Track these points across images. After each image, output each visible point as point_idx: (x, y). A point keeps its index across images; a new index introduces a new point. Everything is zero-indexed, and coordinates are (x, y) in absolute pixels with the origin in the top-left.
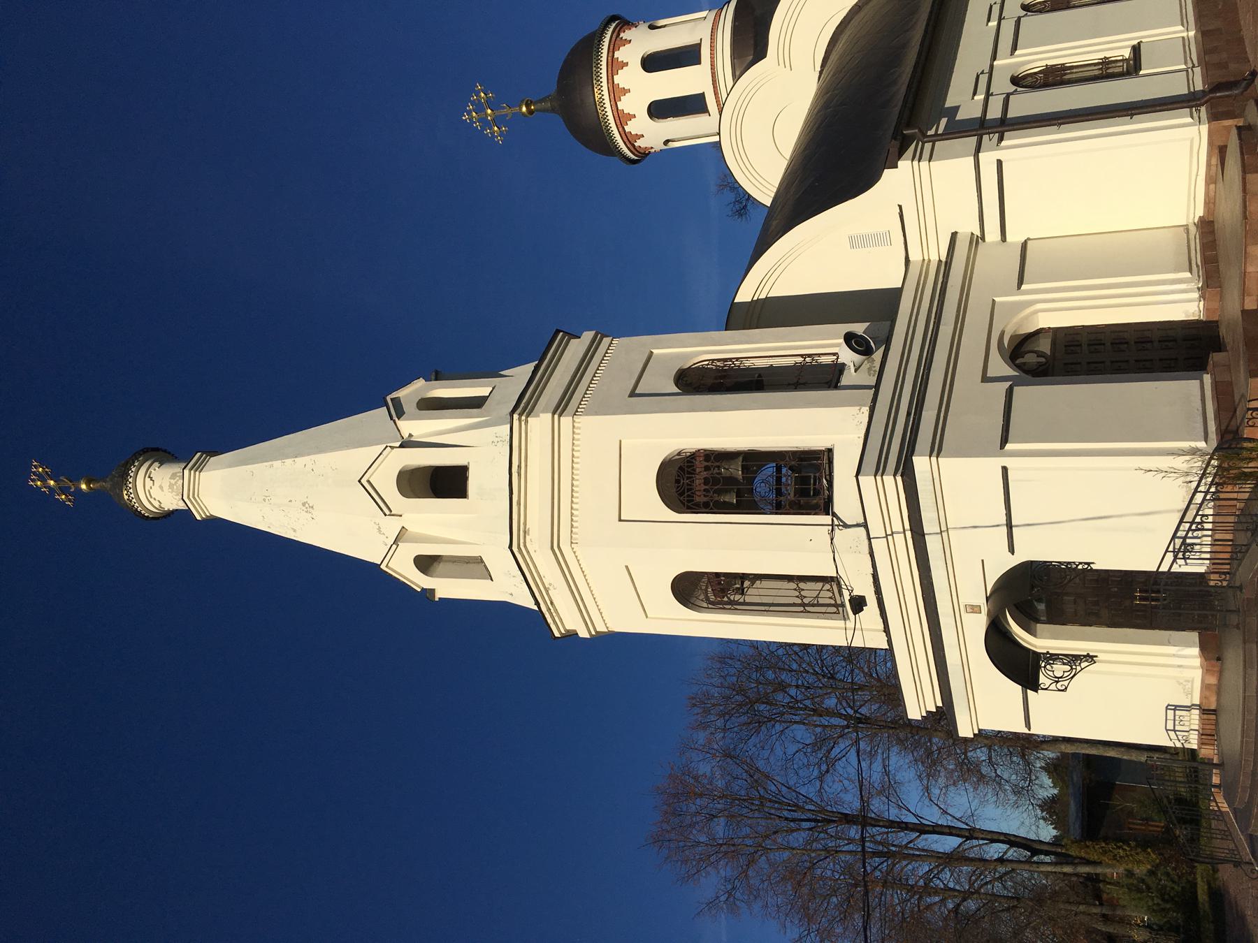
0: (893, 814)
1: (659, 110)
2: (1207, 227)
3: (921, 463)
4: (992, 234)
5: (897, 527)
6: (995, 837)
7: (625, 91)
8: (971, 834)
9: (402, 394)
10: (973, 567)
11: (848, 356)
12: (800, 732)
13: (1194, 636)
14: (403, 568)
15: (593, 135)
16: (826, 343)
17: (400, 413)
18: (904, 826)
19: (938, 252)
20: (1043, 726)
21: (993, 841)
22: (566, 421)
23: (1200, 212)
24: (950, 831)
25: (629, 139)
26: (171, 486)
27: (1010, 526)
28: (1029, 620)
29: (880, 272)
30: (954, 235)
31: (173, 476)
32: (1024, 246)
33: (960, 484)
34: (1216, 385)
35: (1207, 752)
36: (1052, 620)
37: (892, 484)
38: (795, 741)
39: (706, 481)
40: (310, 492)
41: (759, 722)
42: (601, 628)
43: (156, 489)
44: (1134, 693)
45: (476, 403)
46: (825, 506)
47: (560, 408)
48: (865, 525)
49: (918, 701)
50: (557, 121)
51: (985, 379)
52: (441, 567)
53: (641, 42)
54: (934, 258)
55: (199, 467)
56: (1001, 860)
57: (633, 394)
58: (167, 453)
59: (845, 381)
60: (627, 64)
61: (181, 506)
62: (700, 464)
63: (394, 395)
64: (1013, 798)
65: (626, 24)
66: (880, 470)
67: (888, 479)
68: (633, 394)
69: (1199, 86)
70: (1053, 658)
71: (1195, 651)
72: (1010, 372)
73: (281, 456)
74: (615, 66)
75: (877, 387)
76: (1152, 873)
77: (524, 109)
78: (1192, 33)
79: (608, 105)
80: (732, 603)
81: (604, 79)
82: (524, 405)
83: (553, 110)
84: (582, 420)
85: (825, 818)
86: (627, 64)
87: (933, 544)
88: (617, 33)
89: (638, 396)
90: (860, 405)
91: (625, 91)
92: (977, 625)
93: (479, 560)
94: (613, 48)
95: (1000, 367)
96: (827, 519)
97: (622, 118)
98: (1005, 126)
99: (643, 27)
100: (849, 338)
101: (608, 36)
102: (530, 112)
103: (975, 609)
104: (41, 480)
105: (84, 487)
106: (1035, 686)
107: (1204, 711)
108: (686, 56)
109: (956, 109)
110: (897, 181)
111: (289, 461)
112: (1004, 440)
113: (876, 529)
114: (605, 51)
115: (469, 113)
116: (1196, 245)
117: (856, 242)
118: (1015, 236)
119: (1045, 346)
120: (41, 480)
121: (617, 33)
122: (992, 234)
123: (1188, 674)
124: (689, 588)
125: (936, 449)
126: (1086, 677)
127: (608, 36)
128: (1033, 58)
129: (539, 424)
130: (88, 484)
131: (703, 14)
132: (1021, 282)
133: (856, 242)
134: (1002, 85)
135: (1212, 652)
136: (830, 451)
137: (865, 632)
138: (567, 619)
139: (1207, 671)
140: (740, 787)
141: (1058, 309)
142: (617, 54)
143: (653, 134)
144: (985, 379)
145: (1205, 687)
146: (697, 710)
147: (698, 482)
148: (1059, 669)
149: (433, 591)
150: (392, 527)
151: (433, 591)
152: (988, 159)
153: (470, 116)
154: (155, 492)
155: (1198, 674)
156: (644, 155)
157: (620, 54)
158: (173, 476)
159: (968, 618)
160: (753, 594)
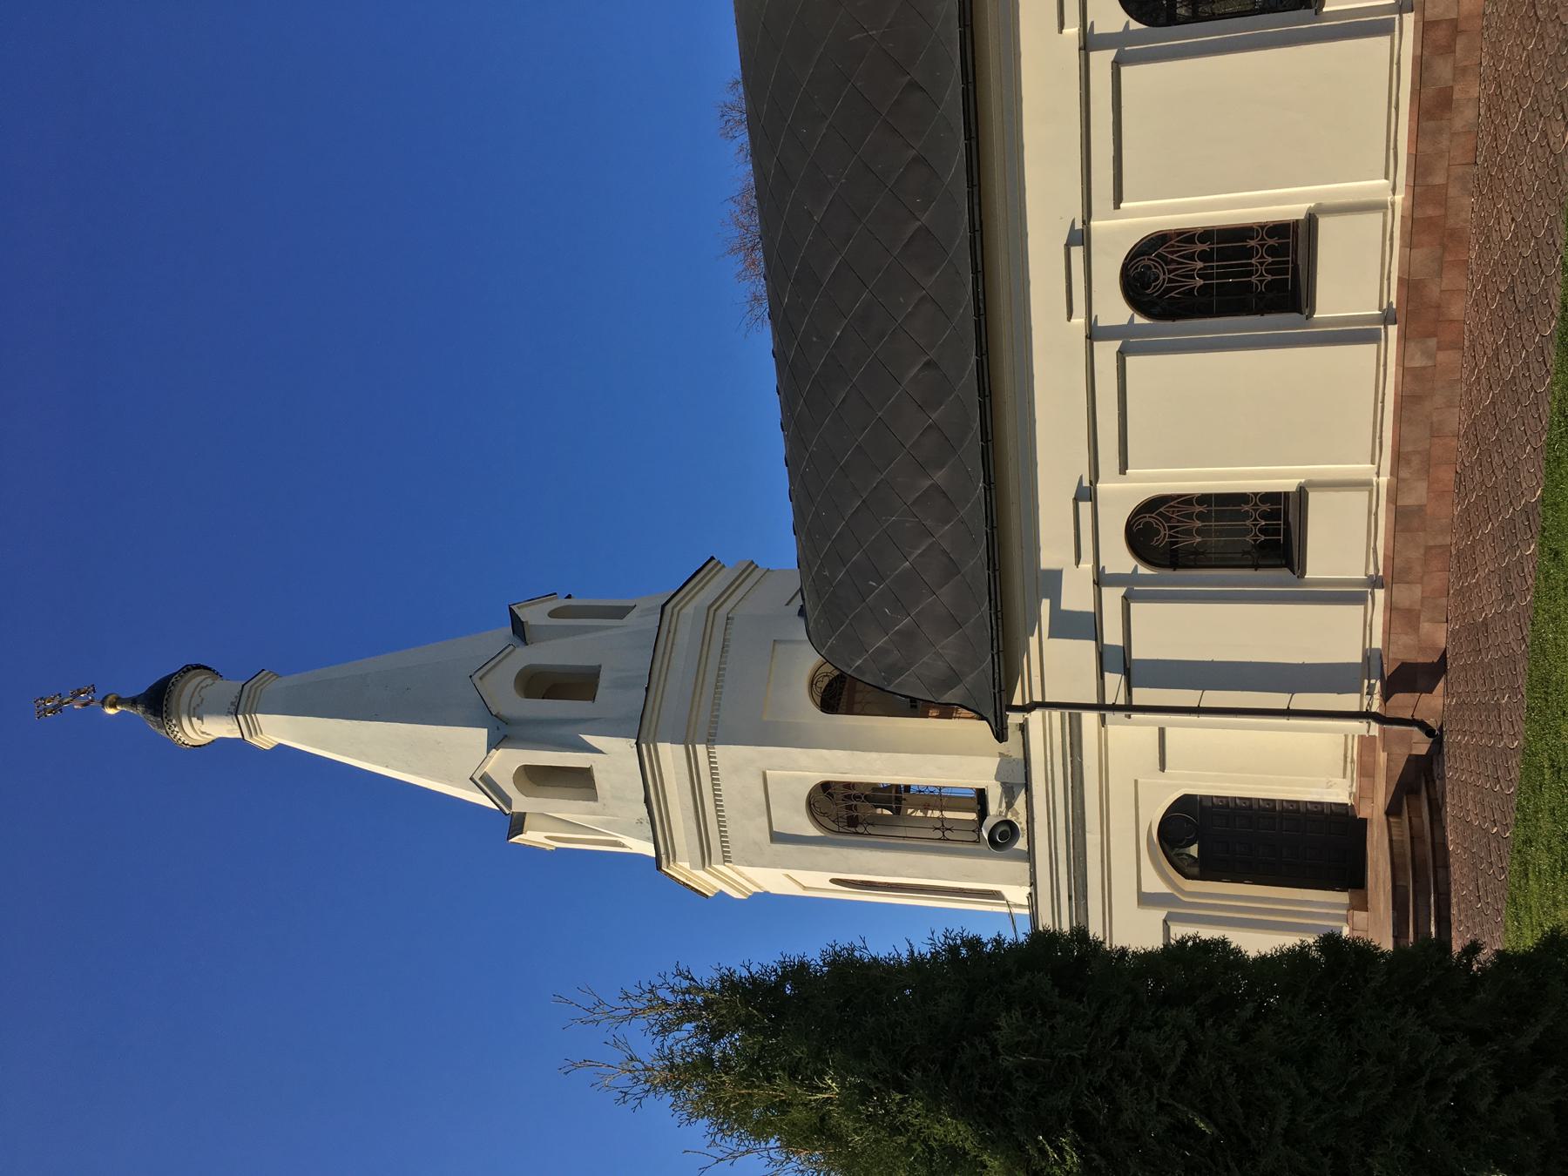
22: (720, 867)
51: (1145, 900)
68: (777, 837)
69: (1377, 643)
75: (1030, 856)
78: (1384, 480)
90: (1021, 885)
95: (1154, 883)
105: (111, 711)
109: (1057, 575)
130: (113, 706)
132: (1163, 767)
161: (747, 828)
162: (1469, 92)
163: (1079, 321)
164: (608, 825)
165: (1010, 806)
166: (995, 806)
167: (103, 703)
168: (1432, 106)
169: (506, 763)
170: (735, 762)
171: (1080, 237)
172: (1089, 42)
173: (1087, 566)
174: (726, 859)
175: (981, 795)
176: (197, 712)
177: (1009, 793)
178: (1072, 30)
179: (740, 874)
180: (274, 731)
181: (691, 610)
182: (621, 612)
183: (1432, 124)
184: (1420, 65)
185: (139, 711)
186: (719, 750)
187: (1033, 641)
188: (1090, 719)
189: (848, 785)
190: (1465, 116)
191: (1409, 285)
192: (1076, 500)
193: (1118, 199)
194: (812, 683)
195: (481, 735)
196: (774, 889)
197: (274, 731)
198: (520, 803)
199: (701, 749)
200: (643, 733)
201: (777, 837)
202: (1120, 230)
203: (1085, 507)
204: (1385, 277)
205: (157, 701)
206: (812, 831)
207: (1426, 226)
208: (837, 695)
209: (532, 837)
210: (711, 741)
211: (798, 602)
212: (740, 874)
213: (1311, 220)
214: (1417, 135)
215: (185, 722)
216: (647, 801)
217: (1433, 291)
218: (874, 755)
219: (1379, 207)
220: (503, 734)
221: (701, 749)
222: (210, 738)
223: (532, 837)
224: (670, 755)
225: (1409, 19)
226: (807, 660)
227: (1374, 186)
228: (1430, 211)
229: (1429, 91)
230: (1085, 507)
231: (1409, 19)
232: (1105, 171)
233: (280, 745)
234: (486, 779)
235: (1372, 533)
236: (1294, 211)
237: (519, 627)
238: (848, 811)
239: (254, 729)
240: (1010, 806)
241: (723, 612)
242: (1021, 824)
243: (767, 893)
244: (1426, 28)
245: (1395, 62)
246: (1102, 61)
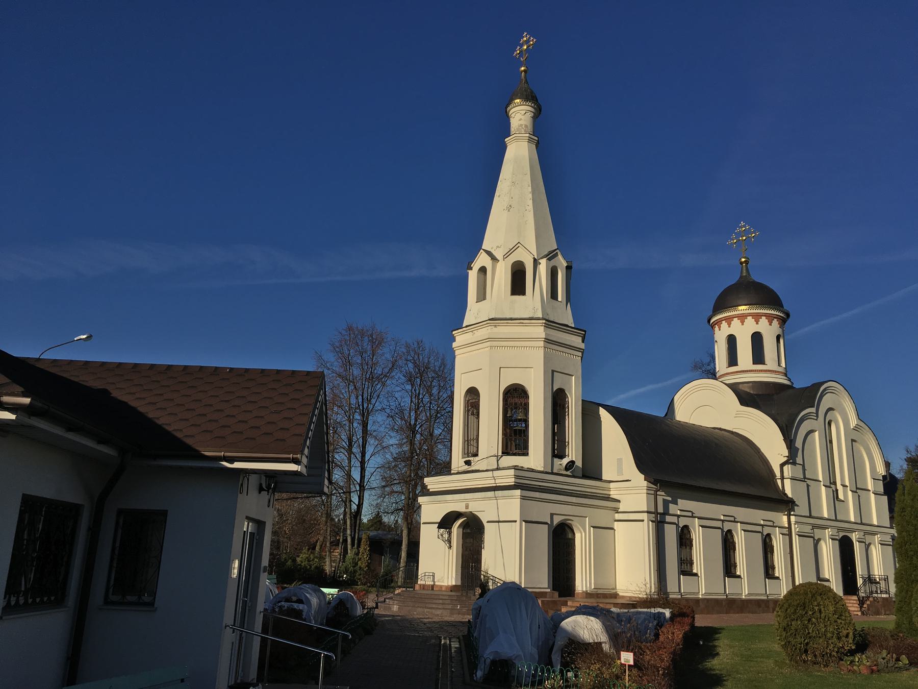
0: (370, 450)
1: (732, 341)
2: (615, 596)
3: (518, 492)
4: (617, 516)
5: (497, 481)
6: (361, 498)
7: (743, 323)
8: (362, 488)
9: (560, 256)
10: (482, 507)
11: (565, 461)
12: (406, 402)
13: (459, 583)
14: (482, 260)
15: (723, 302)
16: (574, 452)
17: (551, 256)
18: (363, 454)
19: (614, 494)
20: (424, 529)
21: (359, 497)
22: (542, 344)
23: (621, 594)
24: (362, 477)
25: (718, 323)
26: (521, 125)
27: (499, 522)
28: (464, 526)
29: (608, 471)
30: (619, 501)
31: (526, 126)
32: (612, 529)
33: (511, 505)
34: (546, 593)
35: (417, 587)
36: (463, 533)
37: (511, 481)
38: (402, 397)
39: (516, 404)
40: (515, 219)
41: (410, 379)
42: (457, 353)
43: (520, 115)
44: (438, 563)
45: (554, 295)
46: (506, 452)
47: (547, 341)
48: (498, 469)
49: (432, 483)
50: (733, 280)
51: (552, 515)
52: (482, 276)
53: (769, 330)
54: (611, 493)
55: (530, 140)
56: (351, 501)
57: (553, 371)
58: (537, 116)
59: (556, 460)
61: (512, 129)
62: (523, 401)
63: (559, 254)
64: (374, 503)
65: (783, 321)
66: (516, 477)
67: (513, 480)
68: (553, 371)
70: (450, 533)
71: (454, 584)
72: (555, 523)
73: (533, 192)
74: (757, 317)
75: (552, 473)
76: (360, 568)
77: (743, 260)
79: (736, 313)
80: (468, 411)
81: (752, 311)
82: (550, 324)
83: (741, 277)
84: (542, 351)
85: (365, 415)
87: (490, 494)
88: (777, 317)
89: (551, 374)
91: (743, 323)
92: (461, 508)
93: (484, 299)
94: (766, 315)
95: (557, 520)
96: (500, 454)
97: (729, 320)
98: (659, 521)
99: (779, 331)
100: (573, 462)
101: (775, 313)
102: (741, 263)
103: (467, 507)
104: (527, 41)
106: (439, 527)
107: (433, 586)
108: (758, 357)
110: (639, 480)
111: (531, 196)
112: (526, 522)
113: (496, 473)
114: (766, 311)
115: (744, 226)
116: (606, 592)
117: (620, 461)
118: (616, 525)
119: (570, 536)
120: (527, 41)
122: (617, 516)
123: (446, 581)
124: (473, 393)
125: (523, 498)
126: (443, 546)
128: (697, 535)
129: (539, 331)
130: (525, 71)
131: (783, 365)
133: (620, 461)
134: (683, 522)
135: (454, 588)
136: (527, 454)
137: (457, 461)
138: (461, 338)
139: (447, 587)
140: (378, 371)
141: (582, 541)
142: (764, 318)
143: (721, 335)
144: (552, 515)
145: (441, 587)
146: (416, 344)
147: (517, 400)
148: (446, 536)
149: (471, 269)
150: (499, 255)
151: (471, 269)
152: (645, 516)
153: (743, 226)
154: (518, 116)
155: (446, 584)
156: (713, 327)
157: (764, 320)
158: (526, 126)
159: (464, 504)
160: (471, 418)
173: (679, 513)
187: (663, 493)
215: (533, 110)
216: (567, 326)
221: (580, 354)
230: (690, 514)
234: (556, 255)
235: (690, 593)
246: (759, 529)
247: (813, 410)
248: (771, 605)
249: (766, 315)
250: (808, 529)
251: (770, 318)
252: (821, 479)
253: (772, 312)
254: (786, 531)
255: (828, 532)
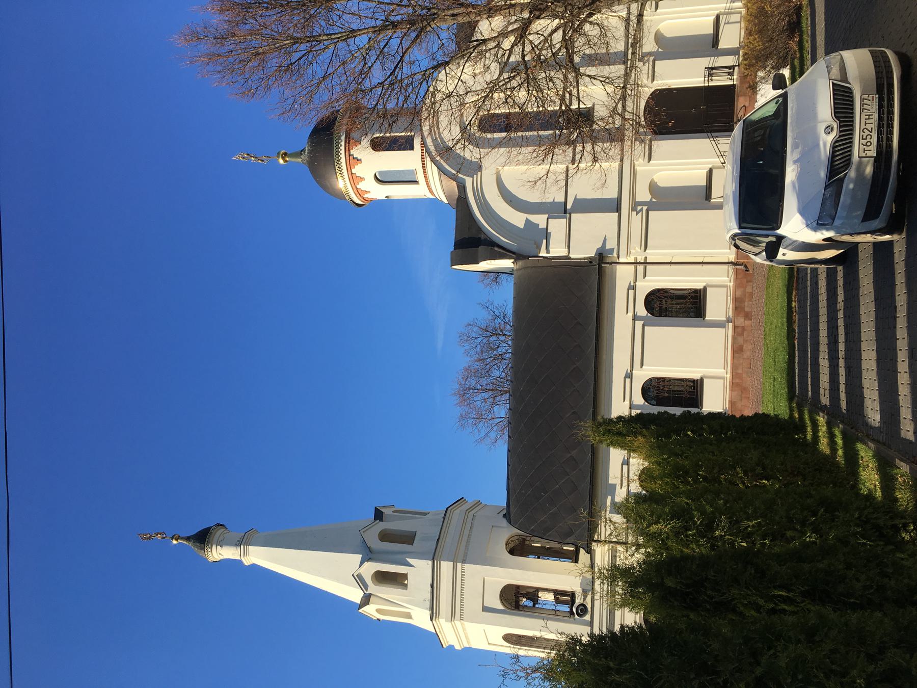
22: (458, 623)
60: (362, 179)
68: (485, 609)
81: (345, 170)
86: (362, 179)
88: (348, 150)
94: (349, 168)
101: (343, 156)
105: (175, 542)
121: (348, 150)
127: (343, 156)
130: (177, 540)
157: (357, 170)
161: (472, 603)
162: (747, 347)
163: (627, 402)
164: (409, 602)
165: (584, 599)
166: (578, 601)
167: (172, 538)
168: (737, 350)
169: (371, 568)
170: (473, 572)
171: (629, 376)
172: (635, 318)
174: (461, 619)
175: (573, 595)
176: (221, 544)
177: (585, 593)
178: (630, 314)
179: (464, 629)
180: (258, 556)
181: (457, 514)
182: (425, 514)
183: (736, 355)
184: (734, 338)
185: (189, 544)
186: (467, 566)
188: (620, 548)
189: (518, 587)
190: (747, 354)
191: (732, 403)
192: (622, 465)
193: (642, 365)
194: (507, 544)
195: (359, 557)
196: (474, 646)
197: (258, 556)
198: (373, 588)
199: (459, 565)
200: (434, 557)
201: (485, 609)
202: (642, 375)
203: (625, 467)
204: (724, 399)
205: (203, 538)
206: (501, 607)
207: (737, 385)
208: (519, 549)
209: (370, 610)
210: (464, 562)
211: (504, 512)
212: (464, 629)
213: (702, 380)
214: (733, 358)
215: (214, 547)
216: (432, 586)
217: (739, 405)
218: (531, 573)
219: (722, 378)
220: (369, 555)
221: (459, 565)
222: (222, 558)
223: (370, 610)
224: (446, 567)
225: (731, 325)
226: (507, 532)
227: (721, 371)
228: (737, 381)
229: (736, 345)
231: (731, 325)
232: (638, 356)
233: (254, 564)
236: (697, 376)
237: (379, 515)
238: (517, 599)
239: (246, 553)
240: (584, 599)
241: (472, 513)
242: (589, 607)
243: (470, 648)
244: (735, 327)
245: (726, 336)
246: (639, 324)
247: (469, 181)
248: (740, 321)
249: (349, 168)
250: (637, 220)
251: (353, 161)
252: (564, 167)
253: (343, 160)
254: (641, 268)
255: (642, 166)
